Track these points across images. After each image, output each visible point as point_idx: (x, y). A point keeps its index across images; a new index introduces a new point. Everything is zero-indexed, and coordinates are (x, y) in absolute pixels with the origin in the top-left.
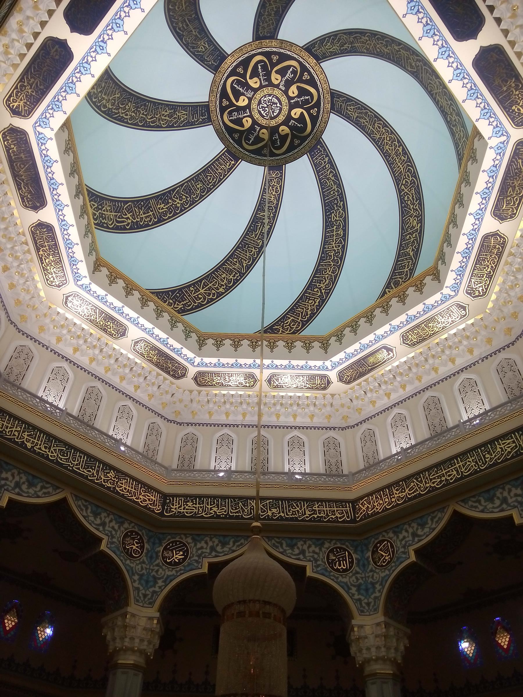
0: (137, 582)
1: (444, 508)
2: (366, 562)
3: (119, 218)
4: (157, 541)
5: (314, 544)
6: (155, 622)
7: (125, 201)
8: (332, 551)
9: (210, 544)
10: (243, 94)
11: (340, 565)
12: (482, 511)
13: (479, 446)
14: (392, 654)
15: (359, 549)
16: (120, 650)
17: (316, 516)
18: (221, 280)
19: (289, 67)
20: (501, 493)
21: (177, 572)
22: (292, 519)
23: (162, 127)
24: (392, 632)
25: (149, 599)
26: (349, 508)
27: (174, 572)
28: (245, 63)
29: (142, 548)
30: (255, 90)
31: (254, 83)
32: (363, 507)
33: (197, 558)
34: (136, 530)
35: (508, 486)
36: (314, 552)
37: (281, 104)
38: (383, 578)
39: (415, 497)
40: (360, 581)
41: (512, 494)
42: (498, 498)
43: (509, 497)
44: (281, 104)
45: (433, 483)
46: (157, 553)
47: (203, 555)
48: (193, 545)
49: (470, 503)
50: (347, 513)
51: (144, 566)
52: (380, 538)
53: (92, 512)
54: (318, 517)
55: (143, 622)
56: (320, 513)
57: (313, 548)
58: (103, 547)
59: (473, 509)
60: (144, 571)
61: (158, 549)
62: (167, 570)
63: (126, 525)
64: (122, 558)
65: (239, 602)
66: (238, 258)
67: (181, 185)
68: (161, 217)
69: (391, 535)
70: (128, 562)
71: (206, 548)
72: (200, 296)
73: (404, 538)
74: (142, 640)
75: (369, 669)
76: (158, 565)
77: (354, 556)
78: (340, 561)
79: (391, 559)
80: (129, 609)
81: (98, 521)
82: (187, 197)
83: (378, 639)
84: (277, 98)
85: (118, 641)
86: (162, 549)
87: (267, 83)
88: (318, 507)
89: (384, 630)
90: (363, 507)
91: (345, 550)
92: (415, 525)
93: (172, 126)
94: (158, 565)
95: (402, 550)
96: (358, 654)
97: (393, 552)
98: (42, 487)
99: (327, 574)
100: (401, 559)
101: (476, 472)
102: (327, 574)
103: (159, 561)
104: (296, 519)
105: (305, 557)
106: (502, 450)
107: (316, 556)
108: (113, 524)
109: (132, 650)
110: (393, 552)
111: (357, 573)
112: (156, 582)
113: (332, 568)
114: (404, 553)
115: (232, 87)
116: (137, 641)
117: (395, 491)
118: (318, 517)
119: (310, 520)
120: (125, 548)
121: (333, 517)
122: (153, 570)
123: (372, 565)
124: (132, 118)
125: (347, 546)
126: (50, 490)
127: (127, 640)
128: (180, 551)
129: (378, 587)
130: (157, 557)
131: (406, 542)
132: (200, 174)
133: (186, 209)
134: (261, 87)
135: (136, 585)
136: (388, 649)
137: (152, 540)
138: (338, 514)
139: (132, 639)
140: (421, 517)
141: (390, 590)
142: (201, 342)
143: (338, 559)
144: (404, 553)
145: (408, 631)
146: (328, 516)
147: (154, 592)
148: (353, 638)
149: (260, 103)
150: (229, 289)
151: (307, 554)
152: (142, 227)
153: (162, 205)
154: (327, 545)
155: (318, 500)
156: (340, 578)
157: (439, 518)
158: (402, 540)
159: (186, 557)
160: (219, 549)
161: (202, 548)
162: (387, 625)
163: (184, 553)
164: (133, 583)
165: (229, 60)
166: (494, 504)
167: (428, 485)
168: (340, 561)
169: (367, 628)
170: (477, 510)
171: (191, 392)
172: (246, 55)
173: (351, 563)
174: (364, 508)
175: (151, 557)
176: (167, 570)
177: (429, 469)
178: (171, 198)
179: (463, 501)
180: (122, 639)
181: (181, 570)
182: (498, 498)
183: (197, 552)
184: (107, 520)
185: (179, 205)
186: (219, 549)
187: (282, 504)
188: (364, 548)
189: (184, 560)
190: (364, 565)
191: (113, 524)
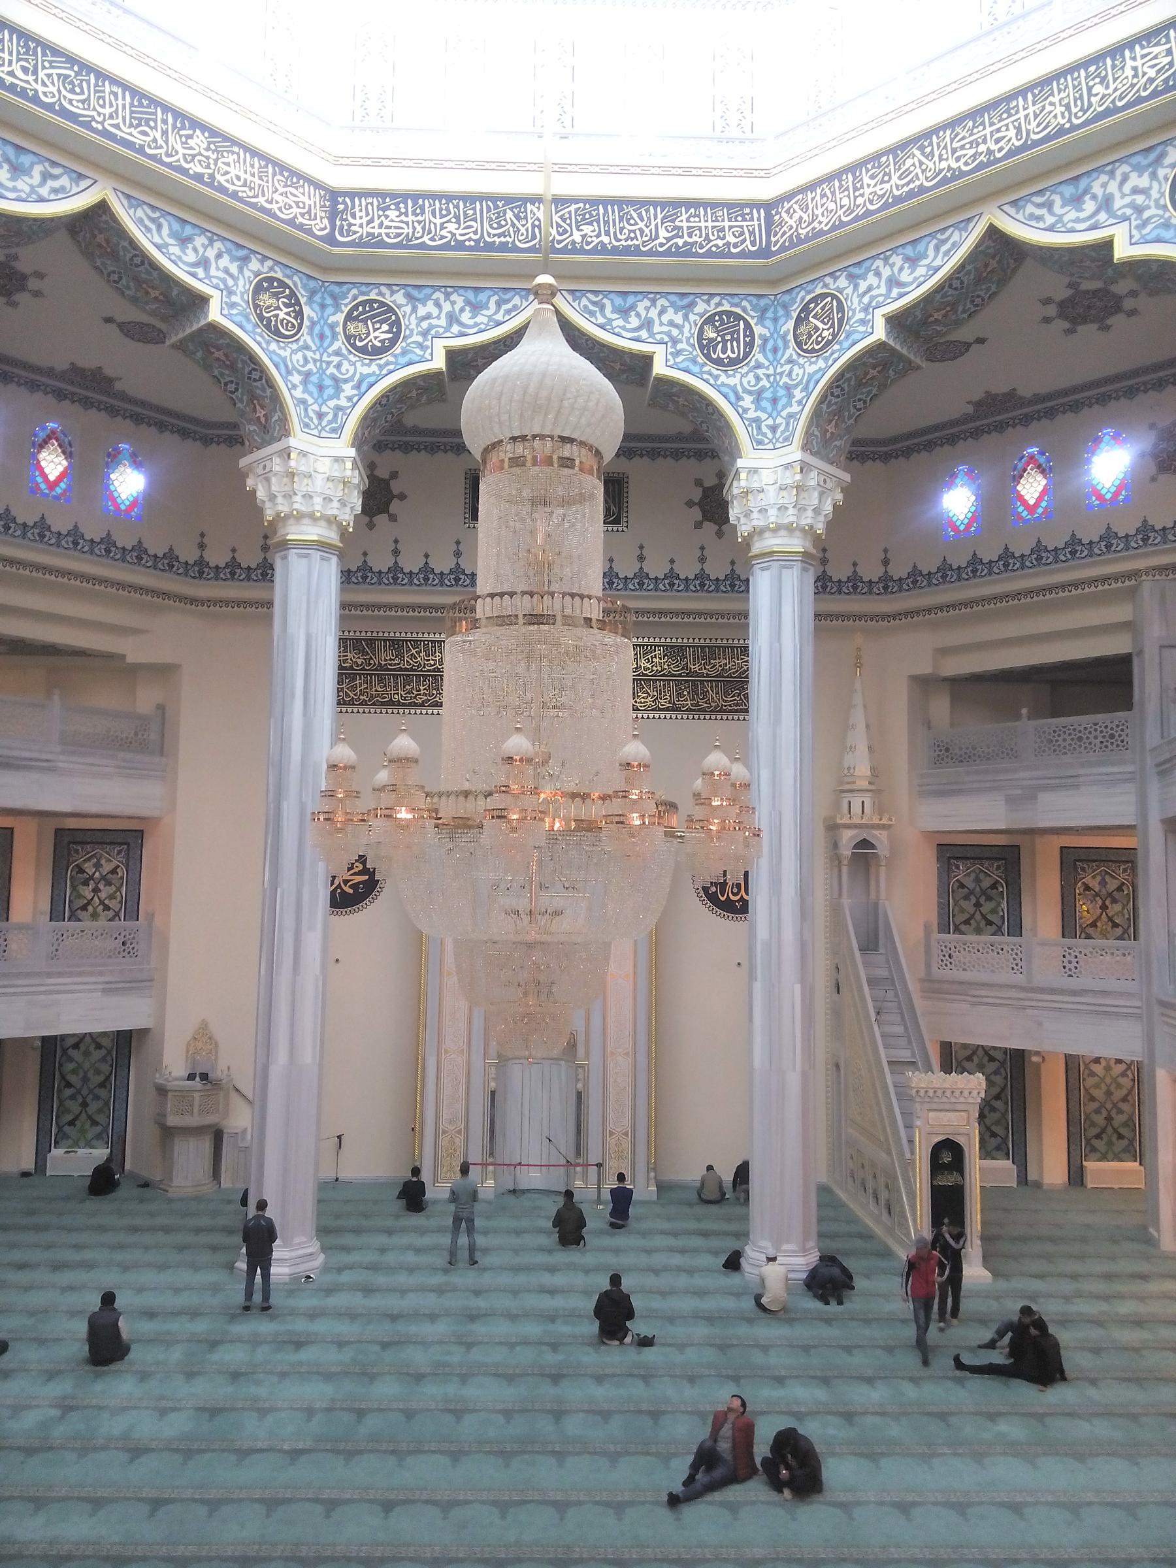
0: (300, 388)
1: (969, 220)
2: (780, 343)
4: (329, 301)
5: (673, 305)
6: (349, 465)
8: (710, 321)
9: (447, 307)
11: (724, 351)
12: (1051, 229)
13: (1085, 63)
14: (807, 520)
15: (770, 314)
20: (1104, 185)
21: (380, 367)
22: (626, 251)
24: (813, 479)
25: (330, 422)
26: (758, 219)
27: (374, 368)
29: (299, 314)
32: (791, 220)
33: (420, 339)
34: (279, 275)
35: (1125, 168)
36: (671, 323)
38: (811, 376)
39: (911, 194)
41: (1127, 188)
42: (1094, 197)
43: (1117, 195)
45: (958, 159)
46: (332, 327)
47: (433, 332)
48: (408, 309)
49: (1030, 209)
50: (752, 233)
51: (309, 354)
52: (819, 291)
53: (173, 235)
54: (686, 244)
55: (325, 467)
56: (690, 235)
57: (670, 314)
58: (215, 314)
59: (1033, 223)
60: (310, 366)
61: (332, 319)
62: (358, 364)
63: (254, 265)
64: (259, 338)
65: (514, 439)
69: (843, 282)
70: (273, 346)
71: (438, 317)
73: (870, 289)
74: (328, 499)
75: (757, 547)
76: (337, 353)
77: (758, 330)
78: (724, 342)
79: (835, 336)
80: (292, 442)
81: (191, 257)
83: (784, 493)
85: (280, 500)
86: (340, 317)
88: (688, 220)
89: (798, 477)
91: (739, 317)
92: (897, 260)
94: (337, 353)
95: (862, 316)
96: (743, 520)
97: (841, 321)
98: (46, 176)
99: (695, 369)
100: (857, 336)
101: (1061, 131)
102: (695, 369)
103: (340, 343)
104: (637, 251)
105: (652, 335)
106: (1136, 76)
107: (675, 332)
108: (225, 261)
109: (312, 516)
110: (841, 321)
111: (759, 366)
112: (338, 390)
113: (707, 356)
114: (863, 322)
116: (318, 500)
117: (866, 180)
118: (686, 244)
120: (261, 317)
121: (720, 243)
122: (329, 363)
123: (791, 351)
125: (744, 310)
126: (64, 181)
128: (381, 322)
129: (798, 394)
130: (334, 336)
131: (872, 298)
135: (298, 393)
136: (802, 509)
137: (317, 298)
139: (308, 496)
140: (914, 242)
141: (823, 399)
143: (723, 337)
144: (863, 322)
145: (847, 477)
147: (338, 408)
148: (735, 491)
151: (657, 328)
154: (701, 307)
155: (689, 204)
156: (723, 378)
157: (954, 244)
158: (865, 293)
159: (397, 336)
160: (466, 317)
161: (428, 316)
162: (804, 468)
163: (391, 325)
164: (291, 392)
166: (1081, 210)
167: (944, 165)
168: (724, 342)
169: (764, 473)
170: (1041, 225)
173: (750, 345)
174: (791, 222)
175: (322, 337)
176: (358, 364)
177: (953, 123)
179: (1014, 203)
181: (387, 364)
182: (1094, 197)
183: (418, 325)
184: (211, 253)
186: (466, 317)
188: (781, 312)
189: (393, 342)
190: (775, 350)
191: (225, 261)
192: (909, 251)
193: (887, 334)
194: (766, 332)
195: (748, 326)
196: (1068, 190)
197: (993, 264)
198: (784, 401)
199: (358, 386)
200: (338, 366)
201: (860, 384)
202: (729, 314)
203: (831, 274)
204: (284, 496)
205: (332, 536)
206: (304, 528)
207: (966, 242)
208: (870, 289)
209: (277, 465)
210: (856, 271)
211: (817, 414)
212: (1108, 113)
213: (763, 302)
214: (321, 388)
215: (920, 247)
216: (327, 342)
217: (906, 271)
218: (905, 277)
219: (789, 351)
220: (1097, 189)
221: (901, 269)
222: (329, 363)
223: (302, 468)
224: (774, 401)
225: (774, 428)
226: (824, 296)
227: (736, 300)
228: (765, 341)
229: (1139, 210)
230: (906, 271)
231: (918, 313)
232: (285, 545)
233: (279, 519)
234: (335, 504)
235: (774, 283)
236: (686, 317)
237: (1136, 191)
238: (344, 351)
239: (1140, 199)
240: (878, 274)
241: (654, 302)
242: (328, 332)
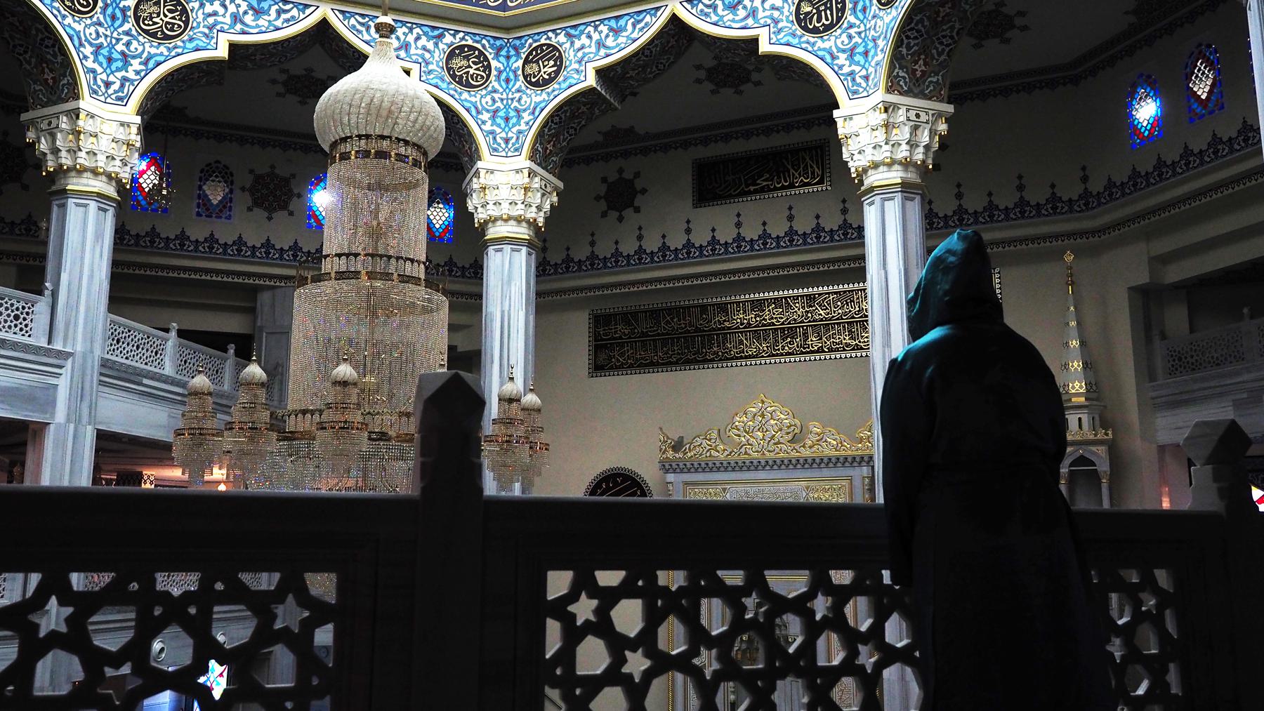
0: (92, 58)
1: (658, 9)
2: (512, 76)
15: (503, 53)
16: (69, 169)
25: (116, 92)
36: (424, 48)
38: (537, 104)
40: (499, 104)
47: (218, 27)
51: (101, 30)
57: (423, 41)
60: (102, 40)
62: (147, 45)
64: (55, 12)
71: (224, 16)
73: (583, 47)
76: (127, 33)
85: (63, 154)
94: (127, 33)
95: (576, 66)
107: (427, 55)
111: (495, 91)
116: (101, 158)
125: (484, 46)
127: (82, 154)
135: (90, 64)
139: (92, 153)
140: (618, 18)
141: (545, 124)
145: (561, 185)
151: (413, 51)
154: (448, 39)
157: (646, 24)
158: (579, 50)
164: (84, 62)
175: (114, 18)
176: (147, 45)
180: (73, 152)
181: (175, 47)
183: (204, 19)
186: (249, 19)
188: (512, 52)
190: (508, 81)
197: (673, 42)
198: (514, 120)
199: (146, 63)
200: (128, 44)
201: (573, 116)
203: (553, 31)
204: (68, 151)
205: (111, 191)
206: (84, 181)
208: (583, 47)
209: (64, 123)
210: (572, 32)
211: (540, 135)
213: (498, 43)
214: (110, 60)
215: (622, 22)
216: (118, 23)
217: (611, 39)
218: (610, 42)
219: (518, 84)
221: (607, 36)
222: (118, 40)
223: (89, 128)
224: (507, 119)
225: (507, 141)
227: (477, 38)
228: (500, 72)
230: (611, 39)
231: (619, 70)
232: (64, 193)
233: (61, 172)
234: (118, 163)
235: (507, 30)
236: (436, 44)
238: (134, 32)
240: (589, 37)
241: (411, 29)
242: (119, 14)
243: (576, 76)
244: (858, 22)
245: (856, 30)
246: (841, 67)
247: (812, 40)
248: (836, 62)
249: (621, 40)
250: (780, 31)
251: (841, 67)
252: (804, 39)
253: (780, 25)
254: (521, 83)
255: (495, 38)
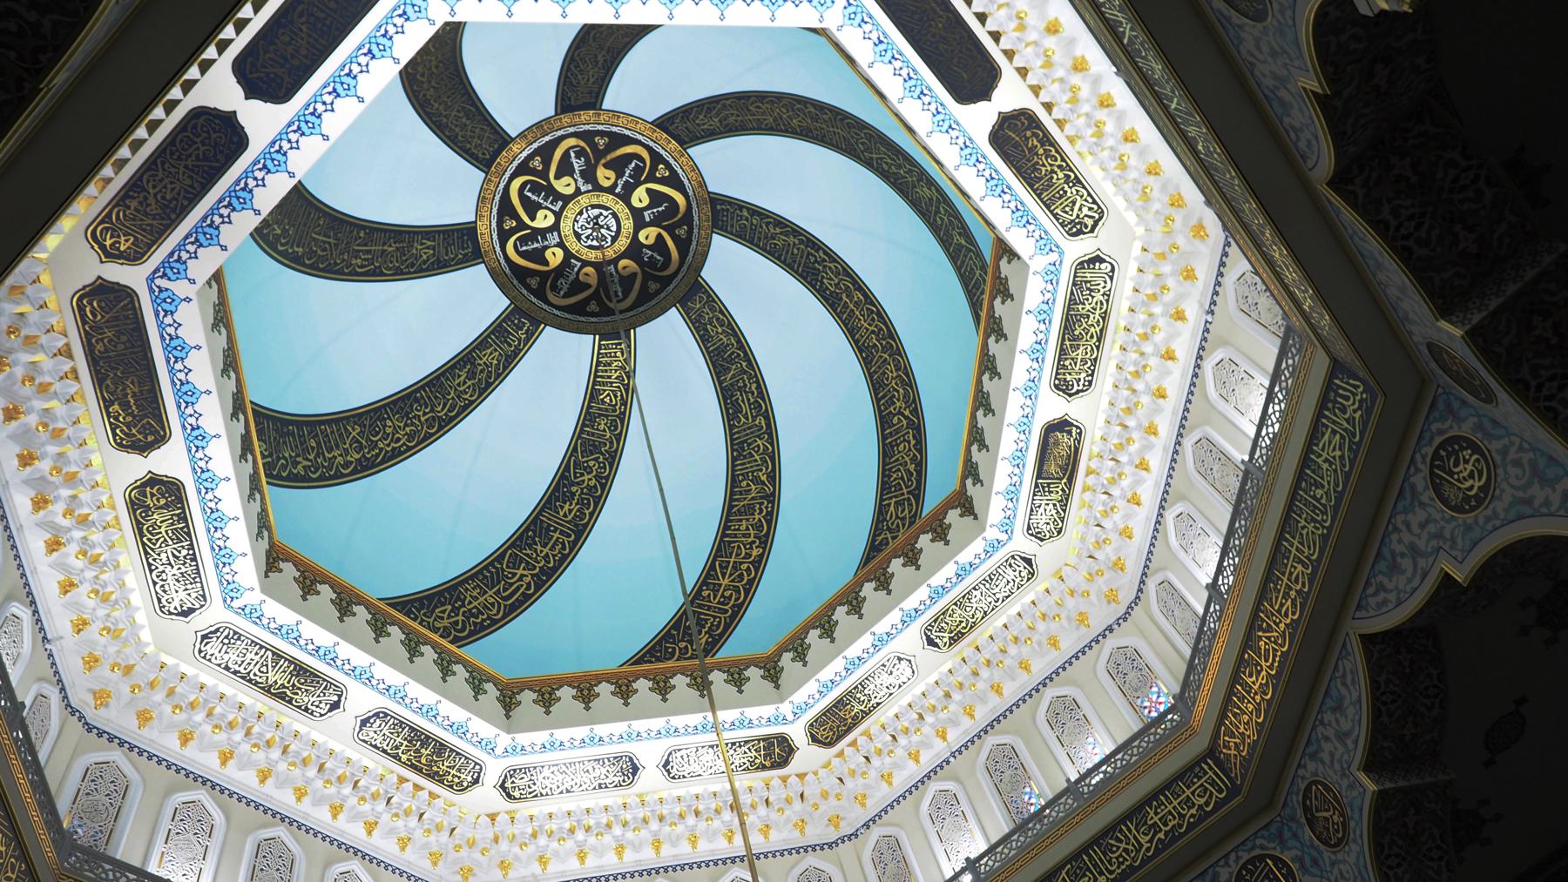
1: (1344, 646)
3: (505, 590)
7: (498, 556)
10: (547, 247)
13: (1296, 486)
15: (1287, 834)
17: (1161, 835)
18: (744, 536)
19: (566, 154)
20: (1400, 541)
23: (472, 402)
26: (1210, 770)
28: (506, 209)
30: (556, 227)
31: (543, 220)
35: (1400, 519)
37: (607, 209)
41: (1416, 529)
42: (1403, 555)
43: (1415, 539)
44: (607, 209)
45: (1286, 615)
49: (1372, 601)
50: (1213, 784)
52: (1303, 786)
54: (1166, 833)
56: (1166, 824)
59: (1384, 609)
66: (745, 476)
67: (572, 451)
68: (576, 525)
72: (727, 594)
73: (1332, 755)
79: (1342, 815)
82: (596, 460)
84: (593, 207)
87: (560, 203)
88: (1156, 814)
90: (1232, 749)
93: (489, 385)
95: (1345, 783)
100: (1357, 803)
101: (1325, 538)
106: (1331, 464)
114: (1351, 787)
115: (521, 254)
117: (1249, 681)
118: (1166, 833)
119: (1158, 852)
121: (1193, 811)
124: (410, 437)
125: (1262, 847)
131: (1340, 762)
132: (589, 407)
133: (607, 478)
134: (558, 215)
138: (1199, 797)
142: (773, 673)
144: (1351, 787)
146: (1182, 816)
149: (578, 236)
150: (766, 541)
152: (555, 569)
153: (567, 507)
155: (1152, 798)
165: (482, 228)
166: (1404, 572)
167: (1282, 626)
171: (827, 765)
172: (497, 198)
174: (1233, 752)
178: (573, 484)
179: (1359, 607)
185: (593, 483)
187: (1089, 856)
188: (1294, 826)
192: (1330, 703)
193: (1377, 782)
194: (1295, 853)
195: (1275, 859)
196: (1382, 566)
202: (1251, 861)
203: (1299, 766)
207: (1355, 663)
208: (1332, 755)
210: (1311, 749)
212: (1339, 500)
213: (1273, 829)
215: (1334, 693)
218: (1346, 726)
219: (1326, 855)
220: (1399, 548)
221: (1337, 721)
226: (1308, 789)
227: (1249, 844)
228: (1300, 860)
229: (1439, 535)
230: (1342, 720)
237: (1423, 526)
239: (1432, 528)
240: (1327, 739)
243: (1355, 793)
244: (1506, 441)
245: (1513, 449)
246: (1547, 503)
247: (1489, 512)
248: (1536, 503)
249: (1351, 711)
250: (1453, 541)
251: (1547, 503)
252: (1481, 521)
253: (1447, 534)
254: (1327, 855)
255: (1266, 827)
